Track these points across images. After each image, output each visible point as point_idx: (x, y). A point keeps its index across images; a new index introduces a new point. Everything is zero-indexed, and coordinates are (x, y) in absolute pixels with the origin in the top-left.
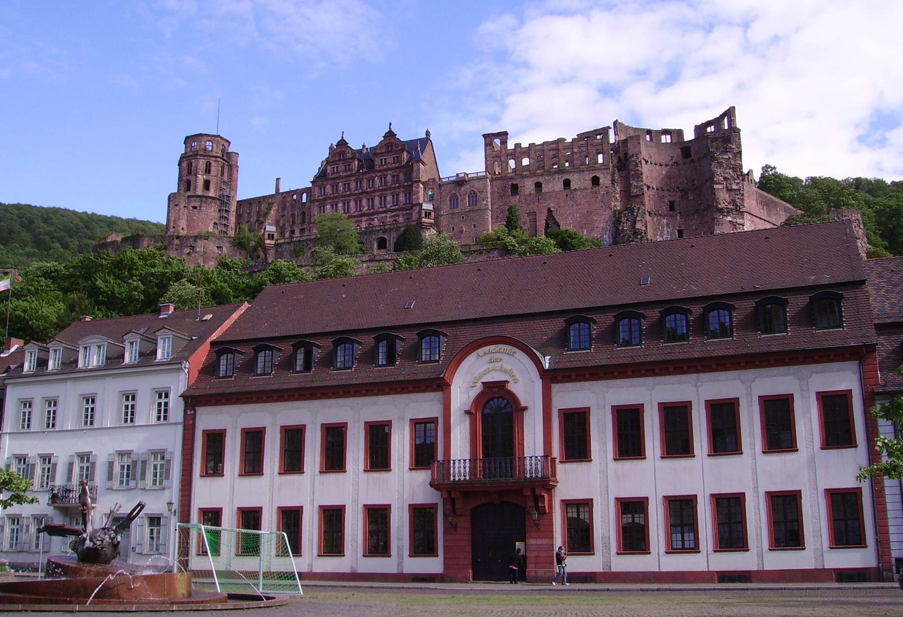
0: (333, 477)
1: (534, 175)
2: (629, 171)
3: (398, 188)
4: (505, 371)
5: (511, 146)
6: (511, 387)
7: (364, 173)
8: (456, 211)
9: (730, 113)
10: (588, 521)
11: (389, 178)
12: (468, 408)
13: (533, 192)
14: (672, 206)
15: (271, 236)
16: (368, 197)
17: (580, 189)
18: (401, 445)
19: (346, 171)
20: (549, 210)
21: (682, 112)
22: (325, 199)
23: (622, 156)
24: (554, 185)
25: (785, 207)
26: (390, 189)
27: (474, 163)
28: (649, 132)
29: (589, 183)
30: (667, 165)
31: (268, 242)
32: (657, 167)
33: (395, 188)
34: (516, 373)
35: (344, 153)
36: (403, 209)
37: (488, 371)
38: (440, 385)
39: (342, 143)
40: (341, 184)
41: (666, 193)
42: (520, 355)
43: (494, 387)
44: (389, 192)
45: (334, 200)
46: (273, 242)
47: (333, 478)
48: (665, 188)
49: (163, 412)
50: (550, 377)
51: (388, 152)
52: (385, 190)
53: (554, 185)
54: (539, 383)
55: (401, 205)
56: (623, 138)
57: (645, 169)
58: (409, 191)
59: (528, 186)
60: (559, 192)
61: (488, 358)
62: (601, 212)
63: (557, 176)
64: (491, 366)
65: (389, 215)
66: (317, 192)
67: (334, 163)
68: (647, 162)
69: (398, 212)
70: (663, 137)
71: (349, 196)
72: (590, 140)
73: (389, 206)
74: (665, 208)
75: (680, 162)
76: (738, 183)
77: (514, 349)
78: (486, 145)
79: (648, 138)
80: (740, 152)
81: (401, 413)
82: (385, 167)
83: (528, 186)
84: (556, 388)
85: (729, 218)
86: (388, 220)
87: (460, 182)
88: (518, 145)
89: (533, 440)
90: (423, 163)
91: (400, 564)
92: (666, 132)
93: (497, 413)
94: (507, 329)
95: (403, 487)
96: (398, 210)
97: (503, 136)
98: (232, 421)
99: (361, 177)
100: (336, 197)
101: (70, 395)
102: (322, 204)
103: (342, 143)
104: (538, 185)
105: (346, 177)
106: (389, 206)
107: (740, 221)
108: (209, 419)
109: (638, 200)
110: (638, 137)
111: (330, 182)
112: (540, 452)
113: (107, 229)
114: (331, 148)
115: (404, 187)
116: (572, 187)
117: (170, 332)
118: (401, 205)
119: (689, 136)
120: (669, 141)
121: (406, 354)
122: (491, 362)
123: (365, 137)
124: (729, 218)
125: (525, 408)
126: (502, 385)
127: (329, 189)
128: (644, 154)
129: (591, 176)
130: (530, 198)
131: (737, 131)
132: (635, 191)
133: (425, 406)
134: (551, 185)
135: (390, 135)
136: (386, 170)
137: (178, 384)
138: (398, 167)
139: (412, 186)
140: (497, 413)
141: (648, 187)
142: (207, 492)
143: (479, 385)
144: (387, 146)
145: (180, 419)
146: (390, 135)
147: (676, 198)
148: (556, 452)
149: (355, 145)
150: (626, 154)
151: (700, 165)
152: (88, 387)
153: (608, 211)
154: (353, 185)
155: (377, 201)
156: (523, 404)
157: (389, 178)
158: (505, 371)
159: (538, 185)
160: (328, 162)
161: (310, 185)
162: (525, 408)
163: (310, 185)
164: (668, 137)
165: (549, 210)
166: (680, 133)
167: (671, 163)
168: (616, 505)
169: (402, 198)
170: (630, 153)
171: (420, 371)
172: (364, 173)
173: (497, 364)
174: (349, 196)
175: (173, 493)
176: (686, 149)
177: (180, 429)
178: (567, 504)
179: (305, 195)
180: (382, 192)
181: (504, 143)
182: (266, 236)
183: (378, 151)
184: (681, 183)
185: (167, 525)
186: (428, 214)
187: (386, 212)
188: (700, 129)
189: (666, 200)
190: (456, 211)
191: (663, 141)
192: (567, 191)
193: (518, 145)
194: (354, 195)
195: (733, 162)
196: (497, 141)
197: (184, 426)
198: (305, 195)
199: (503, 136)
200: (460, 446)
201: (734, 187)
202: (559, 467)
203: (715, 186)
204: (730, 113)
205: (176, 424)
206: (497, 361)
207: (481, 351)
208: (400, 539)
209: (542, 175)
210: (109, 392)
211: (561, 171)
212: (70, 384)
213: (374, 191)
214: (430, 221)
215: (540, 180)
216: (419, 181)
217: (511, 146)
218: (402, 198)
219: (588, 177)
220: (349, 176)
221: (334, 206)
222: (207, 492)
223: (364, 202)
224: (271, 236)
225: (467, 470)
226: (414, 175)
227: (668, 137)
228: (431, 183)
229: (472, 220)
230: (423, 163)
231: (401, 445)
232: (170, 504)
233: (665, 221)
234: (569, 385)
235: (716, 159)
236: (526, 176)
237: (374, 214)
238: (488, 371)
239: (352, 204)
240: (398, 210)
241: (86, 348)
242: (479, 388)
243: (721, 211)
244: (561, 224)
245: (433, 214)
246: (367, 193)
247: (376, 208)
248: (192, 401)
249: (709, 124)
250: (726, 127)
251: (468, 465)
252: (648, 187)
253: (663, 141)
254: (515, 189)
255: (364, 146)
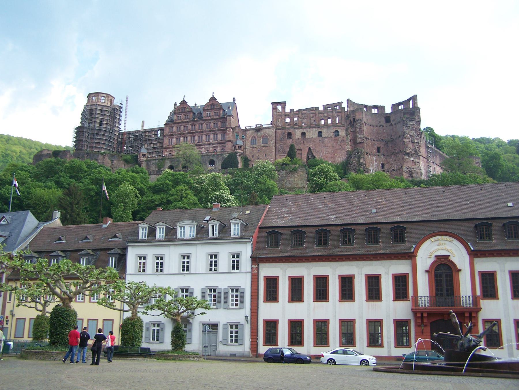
0: (346, 304)
1: (301, 127)
2: (356, 128)
3: (218, 130)
4: (447, 250)
5: (287, 110)
6: (452, 258)
7: (196, 121)
8: (255, 146)
9: (414, 98)
10: (497, 331)
11: (212, 124)
12: (427, 269)
13: (300, 138)
14: (378, 151)
15: (144, 155)
16: (199, 135)
17: (328, 137)
18: (387, 287)
19: (185, 119)
20: (309, 148)
21: (386, 97)
22: (173, 135)
23: (352, 120)
24: (312, 134)
25: (440, 153)
26: (213, 131)
27: (265, 119)
28: (366, 106)
29: (332, 134)
30: (377, 126)
31: (142, 158)
32: (371, 127)
33: (216, 131)
34: (454, 251)
35: (184, 108)
36: (220, 143)
37: (438, 250)
38: (411, 256)
39: (184, 102)
40: (182, 126)
41: (376, 142)
42: (456, 242)
43: (443, 258)
44: (212, 133)
45: (178, 135)
46: (145, 159)
47: (347, 304)
48: (375, 139)
49: (236, 266)
50: (474, 254)
51: (211, 109)
52: (210, 131)
53: (312, 134)
54: (467, 257)
55: (219, 141)
56: (352, 109)
57: (365, 128)
58: (224, 132)
59: (298, 134)
60: (315, 139)
61: (437, 243)
62: (339, 151)
63: (314, 129)
64: (439, 247)
65: (211, 146)
66: (167, 130)
67: (179, 114)
68: (366, 124)
69: (217, 145)
70: (373, 110)
71: (187, 133)
72: (331, 109)
73: (211, 141)
74: (375, 151)
75: (384, 124)
76: (418, 139)
77: (452, 239)
78: (273, 109)
79: (365, 109)
80: (420, 121)
81: (387, 271)
82: (210, 118)
83: (298, 134)
84: (476, 260)
85: (412, 159)
86: (211, 149)
87: (258, 129)
88: (292, 110)
89: (466, 287)
90: (233, 117)
91: (389, 351)
92: (375, 107)
93: (443, 272)
94: (447, 227)
95: (390, 309)
96: (217, 143)
97: (283, 104)
98: (283, 273)
99: (195, 123)
100: (180, 134)
101: (172, 256)
102: (171, 137)
103: (184, 102)
104: (303, 134)
105: (185, 122)
106: (211, 141)
107: (417, 160)
108: (267, 270)
109: (361, 145)
110: (362, 110)
111: (176, 125)
112: (469, 293)
113: (5, 143)
114: (175, 105)
115: (221, 130)
116: (323, 136)
117: (239, 221)
118: (219, 141)
119: (388, 110)
120: (376, 112)
121: (395, 238)
122: (439, 245)
123: (198, 100)
124: (412, 159)
125: (460, 270)
126: (447, 257)
127: (175, 129)
128: (365, 120)
129: (334, 130)
130: (298, 141)
131: (419, 109)
132: (359, 140)
133: (402, 267)
134: (311, 134)
135: (213, 99)
136: (210, 120)
137: (246, 251)
138: (217, 119)
139: (226, 130)
140: (443, 272)
141: (366, 139)
142: (267, 311)
143: (433, 256)
144: (211, 105)
145: (249, 270)
146: (213, 99)
147: (381, 145)
148: (478, 293)
149: (191, 104)
150: (354, 119)
151: (396, 127)
152: (185, 250)
153: (344, 151)
154: (190, 127)
155: (204, 137)
156: (459, 268)
157: (212, 124)
158: (447, 250)
159: (303, 134)
160: (174, 113)
161: (164, 126)
162: (460, 270)
163: (164, 126)
164: (376, 110)
165: (309, 148)
166: (382, 108)
167: (379, 125)
168: (514, 323)
169: (219, 136)
170: (357, 118)
171: (399, 248)
172: (196, 121)
173: (442, 246)
174: (187, 133)
175: (247, 310)
176: (388, 118)
177: (249, 276)
178: (485, 321)
179: (159, 132)
180: (208, 132)
181: (284, 108)
182: (141, 155)
183: (206, 108)
184: (384, 137)
185: (242, 329)
186: (240, 147)
187: (209, 144)
188: (395, 106)
189: (376, 147)
190: (255, 146)
191: (373, 112)
192: (320, 138)
193: (292, 110)
194: (190, 133)
195: (415, 127)
196: (279, 107)
197: (252, 273)
198: (159, 132)
199: (283, 104)
200: (423, 288)
201: (416, 141)
202: (481, 301)
203: (405, 140)
204: (414, 98)
205: (246, 272)
206: (443, 244)
207: (432, 239)
208: (388, 338)
209: (306, 128)
210: (200, 255)
211: (318, 126)
212: (172, 248)
213: (203, 132)
214: (241, 151)
215: (305, 131)
216: (230, 127)
217: (287, 110)
218: (219, 136)
219: (333, 130)
220: (188, 122)
221: (186, 138)
222: (267, 311)
223: (196, 138)
224: (144, 155)
225: (426, 302)
226: (228, 123)
227: (376, 110)
228: (237, 128)
229: (264, 152)
230: (233, 117)
231: (387, 287)
232: (246, 317)
233: (374, 158)
234: (484, 259)
235: (406, 124)
236: (296, 128)
237: (202, 145)
238: (438, 250)
239: (189, 138)
240: (217, 143)
241: (181, 228)
242: (432, 260)
243: (407, 154)
244: (316, 156)
245: (243, 148)
246: (198, 132)
247: (204, 142)
248: (256, 260)
249: (400, 104)
250: (411, 106)
251: (426, 299)
252: (366, 139)
253: (373, 112)
254: (289, 134)
255: (195, 105)
